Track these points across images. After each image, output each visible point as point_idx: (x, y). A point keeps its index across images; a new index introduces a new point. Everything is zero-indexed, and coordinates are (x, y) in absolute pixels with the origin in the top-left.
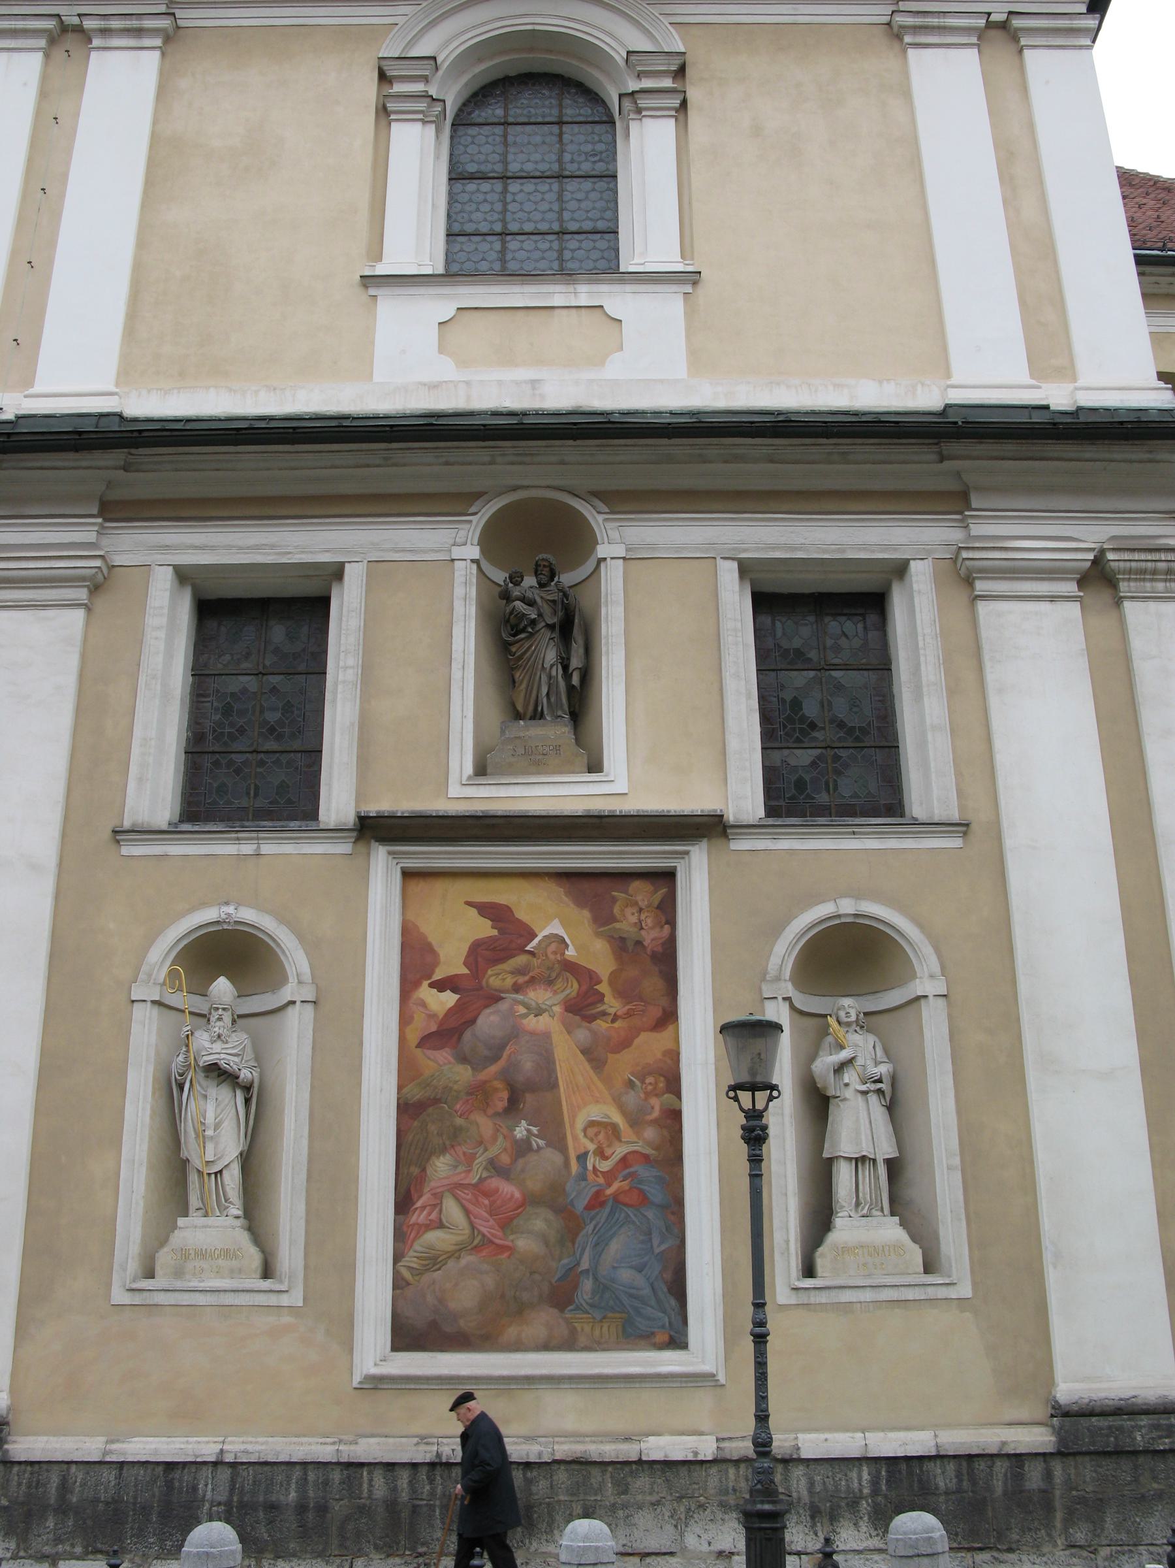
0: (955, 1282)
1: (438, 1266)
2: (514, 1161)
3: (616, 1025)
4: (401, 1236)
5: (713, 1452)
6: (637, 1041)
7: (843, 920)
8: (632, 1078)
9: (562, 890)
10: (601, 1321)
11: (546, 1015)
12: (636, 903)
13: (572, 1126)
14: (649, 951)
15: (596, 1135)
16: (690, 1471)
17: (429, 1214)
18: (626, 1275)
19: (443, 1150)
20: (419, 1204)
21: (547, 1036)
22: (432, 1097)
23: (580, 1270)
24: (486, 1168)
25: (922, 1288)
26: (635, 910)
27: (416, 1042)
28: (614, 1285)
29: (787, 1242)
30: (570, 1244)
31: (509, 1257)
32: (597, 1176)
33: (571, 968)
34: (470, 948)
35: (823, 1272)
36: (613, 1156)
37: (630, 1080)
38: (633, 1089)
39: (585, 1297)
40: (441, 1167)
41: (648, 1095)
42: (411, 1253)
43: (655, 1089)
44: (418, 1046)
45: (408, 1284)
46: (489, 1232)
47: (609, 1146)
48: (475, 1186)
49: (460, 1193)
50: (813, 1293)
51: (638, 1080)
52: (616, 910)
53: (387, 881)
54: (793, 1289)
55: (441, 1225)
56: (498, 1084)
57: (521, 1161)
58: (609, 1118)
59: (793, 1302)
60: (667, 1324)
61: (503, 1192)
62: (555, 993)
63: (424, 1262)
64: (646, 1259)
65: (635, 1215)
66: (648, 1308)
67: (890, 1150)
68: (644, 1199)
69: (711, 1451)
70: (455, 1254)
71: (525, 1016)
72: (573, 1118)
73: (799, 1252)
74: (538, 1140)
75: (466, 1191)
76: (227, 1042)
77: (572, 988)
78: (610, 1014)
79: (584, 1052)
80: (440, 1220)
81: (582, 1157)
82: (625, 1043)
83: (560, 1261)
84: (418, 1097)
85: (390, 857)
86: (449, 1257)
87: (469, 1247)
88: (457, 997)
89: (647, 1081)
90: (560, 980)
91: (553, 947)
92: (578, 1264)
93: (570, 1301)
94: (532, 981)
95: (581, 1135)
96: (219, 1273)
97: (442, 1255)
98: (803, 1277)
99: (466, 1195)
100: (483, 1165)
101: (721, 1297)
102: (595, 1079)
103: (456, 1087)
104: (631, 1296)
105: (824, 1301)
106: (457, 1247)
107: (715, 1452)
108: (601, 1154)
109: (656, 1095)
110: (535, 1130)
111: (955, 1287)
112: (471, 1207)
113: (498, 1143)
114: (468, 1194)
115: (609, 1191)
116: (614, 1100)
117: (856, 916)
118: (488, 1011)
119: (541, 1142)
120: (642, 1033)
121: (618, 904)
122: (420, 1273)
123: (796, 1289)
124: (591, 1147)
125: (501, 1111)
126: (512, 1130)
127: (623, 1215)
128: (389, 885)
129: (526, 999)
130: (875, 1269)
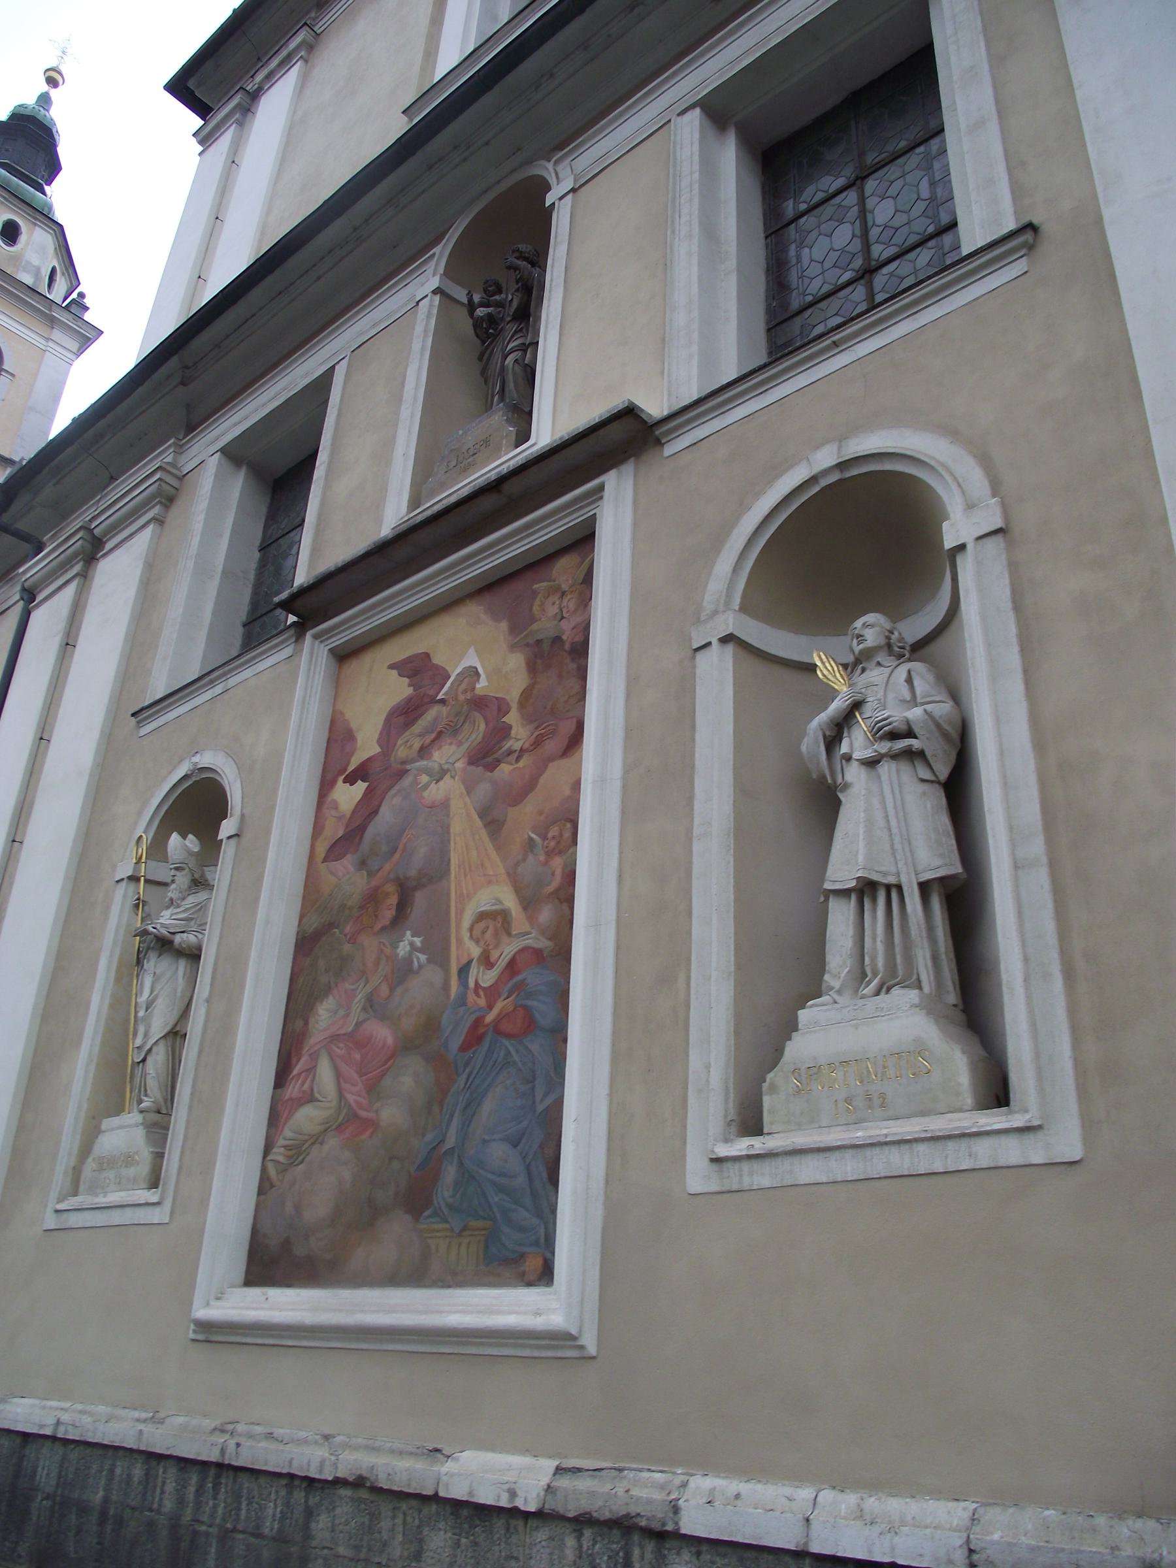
0: (1036, 1123)
1: (301, 1158)
2: (392, 990)
3: (521, 764)
4: (275, 1119)
5: (538, 1495)
6: (542, 780)
7: (824, 482)
8: (533, 835)
9: (482, 608)
10: (460, 1235)
11: (448, 776)
12: (559, 588)
13: (458, 926)
14: (567, 646)
15: (483, 933)
16: (508, 1530)
17: (303, 1083)
18: (499, 1153)
19: (327, 991)
20: (295, 1072)
21: (445, 805)
22: (326, 923)
23: (444, 1150)
24: (364, 1009)
25: (964, 1144)
26: (555, 598)
27: (323, 855)
28: (481, 1171)
29: (708, 1067)
30: (436, 1109)
31: (371, 1136)
32: (478, 995)
33: (480, 703)
34: (385, 721)
35: (772, 1123)
36: (499, 963)
37: (531, 839)
38: (532, 852)
39: (446, 1194)
40: (325, 1015)
41: (549, 854)
42: (281, 1142)
43: (559, 842)
44: (325, 860)
45: (272, 1186)
46: (356, 1101)
47: (496, 946)
48: (350, 1036)
49: (335, 1048)
50: (746, 1166)
51: (539, 837)
52: (536, 608)
53: (309, 670)
54: (713, 1160)
55: (309, 1098)
56: (390, 888)
57: (399, 991)
58: (501, 903)
59: (714, 1188)
60: (542, 1240)
61: (376, 1038)
62: (460, 744)
63: (291, 1153)
64: (524, 1124)
65: (517, 1051)
66: (521, 1209)
67: (937, 862)
68: (530, 1025)
69: (534, 1495)
70: (318, 1139)
71: (426, 786)
72: (461, 912)
73: (731, 1086)
74: (419, 954)
75: (341, 1045)
76: (178, 906)
77: (476, 731)
78: (516, 751)
79: (483, 813)
80: (312, 1090)
81: (464, 971)
82: (531, 785)
83: (424, 1135)
84: (315, 925)
85: (317, 643)
86: (313, 1144)
87: (334, 1127)
88: (366, 784)
89: (550, 835)
90: (467, 724)
91: (463, 686)
92: (442, 1141)
93: (428, 1203)
94: (440, 733)
95: (465, 935)
96: (120, 1185)
97: (306, 1141)
98: (737, 1136)
99: (339, 1050)
100: (362, 1004)
101: (602, 1183)
102: (489, 846)
103: (349, 904)
104: (502, 1189)
105: (766, 1182)
106: (323, 1127)
107: (542, 1493)
108: (487, 961)
109: (560, 853)
110: (418, 941)
111: (1040, 1135)
112: (344, 1068)
113: (379, 970)
114: (342, 1049)
115: (489, 1018)
116: (508, 874)
117: (842, 466)
118: (393, 792)
119: (423, 958)
120: (551, 764)
121: (539, 596)
122: (285, 1170)
123: (717, 1161)
124: (475, 951)
125: (388, 923)
126: (395, 946)
127: (503, 1053)
128: (312, 674)
129: (430, 764)
130: (870, 1107)
